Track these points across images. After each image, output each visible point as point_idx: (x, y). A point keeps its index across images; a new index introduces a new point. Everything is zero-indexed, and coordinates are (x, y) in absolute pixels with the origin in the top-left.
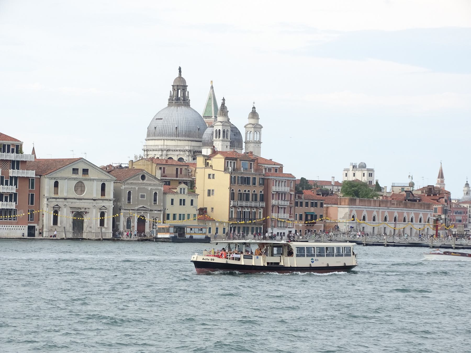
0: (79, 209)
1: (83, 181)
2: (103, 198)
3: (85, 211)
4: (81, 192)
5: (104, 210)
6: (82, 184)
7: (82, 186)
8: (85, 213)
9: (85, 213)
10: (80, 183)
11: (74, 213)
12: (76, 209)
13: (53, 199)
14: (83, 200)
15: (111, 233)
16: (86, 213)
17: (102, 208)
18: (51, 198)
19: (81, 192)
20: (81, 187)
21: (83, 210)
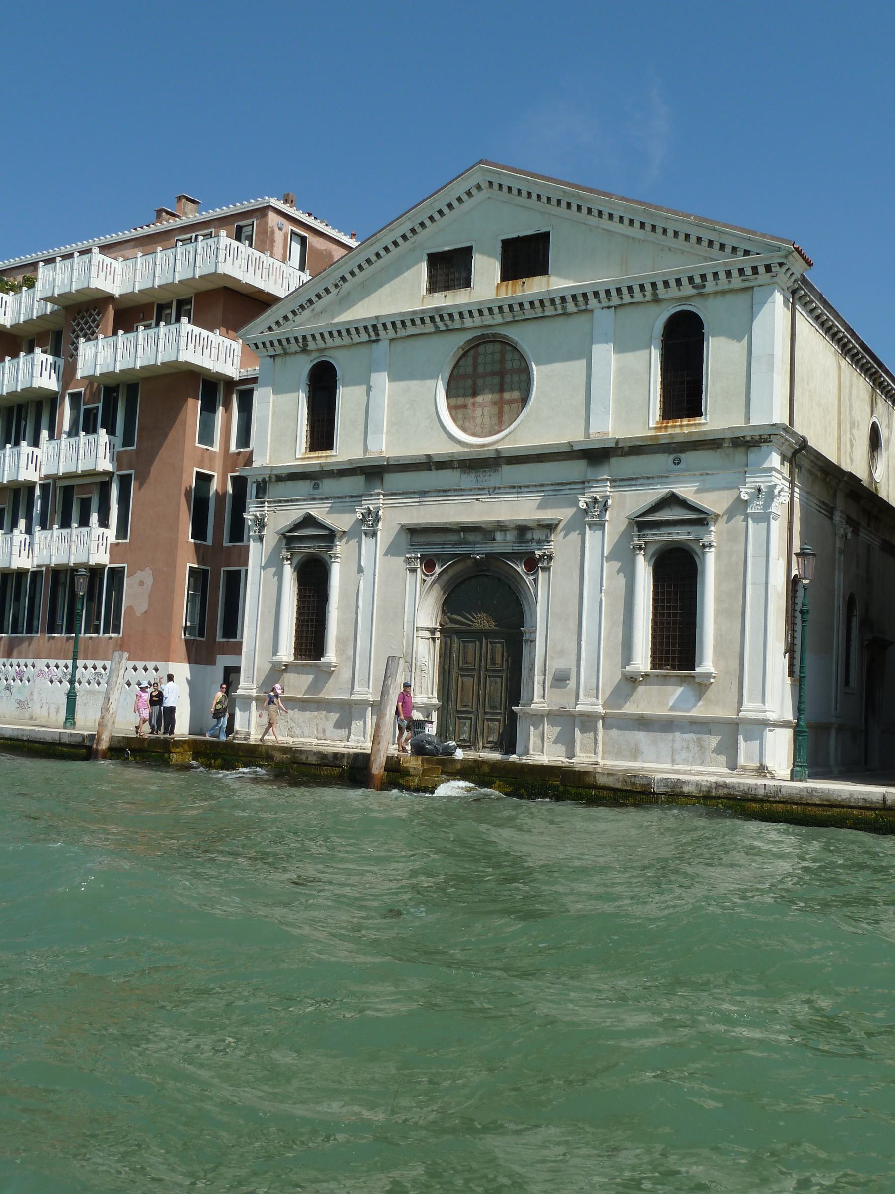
0: (471, 537)
1: (502, 331)
2: (683, 428)
3: (518, 548)
4: (500, 413)
5: (682, 535)
6: (508, 348)
7: (508, 365)
8: (520, 569)
9: (520, 569)
10: (490, 348)
11: (438, 570)
12: (454, 538)
13: (300, 483)
14: (506, 469)
15: (785, 725)
16: (532, 564)
17: (657, 517)
18: (280, 478)
19: (500, 413)
20: (496, 380)
21: (503, 544)
